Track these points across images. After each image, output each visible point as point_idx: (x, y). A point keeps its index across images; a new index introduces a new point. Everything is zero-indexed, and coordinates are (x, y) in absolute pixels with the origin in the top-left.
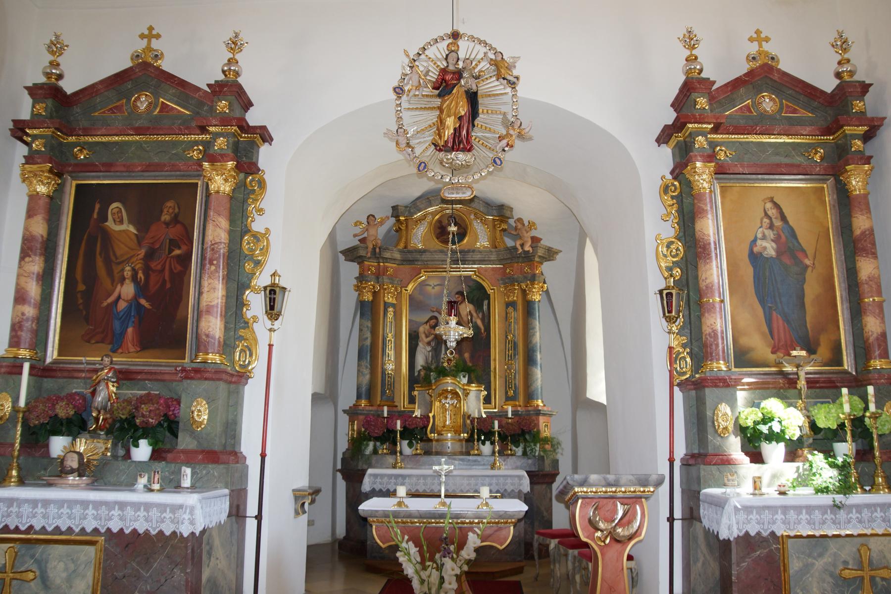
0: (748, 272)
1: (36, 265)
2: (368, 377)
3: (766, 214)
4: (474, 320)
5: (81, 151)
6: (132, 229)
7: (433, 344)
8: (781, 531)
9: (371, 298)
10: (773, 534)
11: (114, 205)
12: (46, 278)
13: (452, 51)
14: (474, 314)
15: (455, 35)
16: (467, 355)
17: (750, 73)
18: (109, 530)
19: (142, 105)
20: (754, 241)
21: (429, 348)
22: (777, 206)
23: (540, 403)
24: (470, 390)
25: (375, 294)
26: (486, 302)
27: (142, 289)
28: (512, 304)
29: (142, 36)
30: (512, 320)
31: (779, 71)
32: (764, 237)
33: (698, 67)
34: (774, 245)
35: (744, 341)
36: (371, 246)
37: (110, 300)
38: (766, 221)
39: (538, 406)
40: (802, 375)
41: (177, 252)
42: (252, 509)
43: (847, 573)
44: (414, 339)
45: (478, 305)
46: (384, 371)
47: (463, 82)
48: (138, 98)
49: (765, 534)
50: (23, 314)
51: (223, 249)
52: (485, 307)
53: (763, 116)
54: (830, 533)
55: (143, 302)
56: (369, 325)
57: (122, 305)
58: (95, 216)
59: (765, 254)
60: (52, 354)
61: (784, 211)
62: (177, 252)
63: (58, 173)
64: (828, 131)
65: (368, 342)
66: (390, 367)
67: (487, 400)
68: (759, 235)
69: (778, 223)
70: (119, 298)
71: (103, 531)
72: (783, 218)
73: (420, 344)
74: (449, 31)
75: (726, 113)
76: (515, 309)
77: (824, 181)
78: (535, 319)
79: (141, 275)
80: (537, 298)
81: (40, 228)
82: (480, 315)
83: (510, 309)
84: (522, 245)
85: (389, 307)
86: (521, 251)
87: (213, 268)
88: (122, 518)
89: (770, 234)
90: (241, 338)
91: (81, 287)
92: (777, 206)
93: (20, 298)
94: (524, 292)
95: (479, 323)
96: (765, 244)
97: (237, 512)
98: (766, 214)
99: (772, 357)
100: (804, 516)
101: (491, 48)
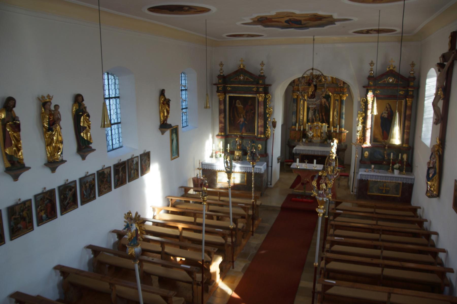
0: (380, 121)
1: (222, 115)
2: (295, 120)
3: (387, 107)
4: (326, 104)
5: (229, 88)
6: (242, 106)
7: (314, 110)
8: (369, 179)
9: (296, 97)
10: (368, 180)
11: (238, 101)
12: (225, 118)
13: (312, 74)
14: (326, 102)
15: (312, 69)
16: (323, 114)
17: (388, 72)
18: (248, 172)
19: (242, 78)
20: (382, 114)
21: (313, 111)
22: (389, 105)
23: (343, 129)
24: (323, 125)
25: (297, 96)
26: (329, 99)
27: (245, 120)
28: (337, 100)
29: (240, 61)
30: (337, 105)
31: (395, 71)
32: (385, 113)
33: (373, 72)
34: (387, 115)
35: (376, 137)
36: (296, 84)
37: (239, 121)
38: (386, 109)
39: (342, 130)
40: (387, 146)
41: (252, 112)
42: (270, 165)
43: (381, 188)
44: (308, 109)
45: (327, 100)
46: (299, 118)
47: (313, 83)
48: (241, 77)
49: (366, 179)
50: (222, 126)
51: (263, 113)
52: (329, 100)
53: (389, 83)
54: (379, 180)
55: (246, 122)
56: (296, 105)
57: (241, 123)
58: (234, 102)
59: (385, 117)
60: (228, 133)
61: (391, 107)
62: (252, 112)
63: (225, 94)
64: (404, 88)
65: (295, 110)
66: (301, 116)
67: (328, 127)
68: (384, 112)
69: (389, 110)
70: (240, 121)
71: (246, 171)
72: (391, 108)
73: (310, 110)
74: (311, 68)
75: (380, 82)
76: (338, 102)
77: (403, 99)
78: (343, 105)
79: (245, 116)
80: (345, 98)
81: (222, 107)
82: (328, 102)
83: (337, 102)
84: (340, 84)
85: (301, 100)
86: (340, 86)
87: (261, 117)
88: (250, 170)
89: (387, 112)
90: (267, 131)
91: (232, 119)
92: (389, 105)
93: (220, 122)
94: (341, 97)
95: (327, 105)
96: (385, 114)
97: (267, 165)
98: (387, 107)
99: (383, 141)
100: (374, 177)
101: (321, 73)
